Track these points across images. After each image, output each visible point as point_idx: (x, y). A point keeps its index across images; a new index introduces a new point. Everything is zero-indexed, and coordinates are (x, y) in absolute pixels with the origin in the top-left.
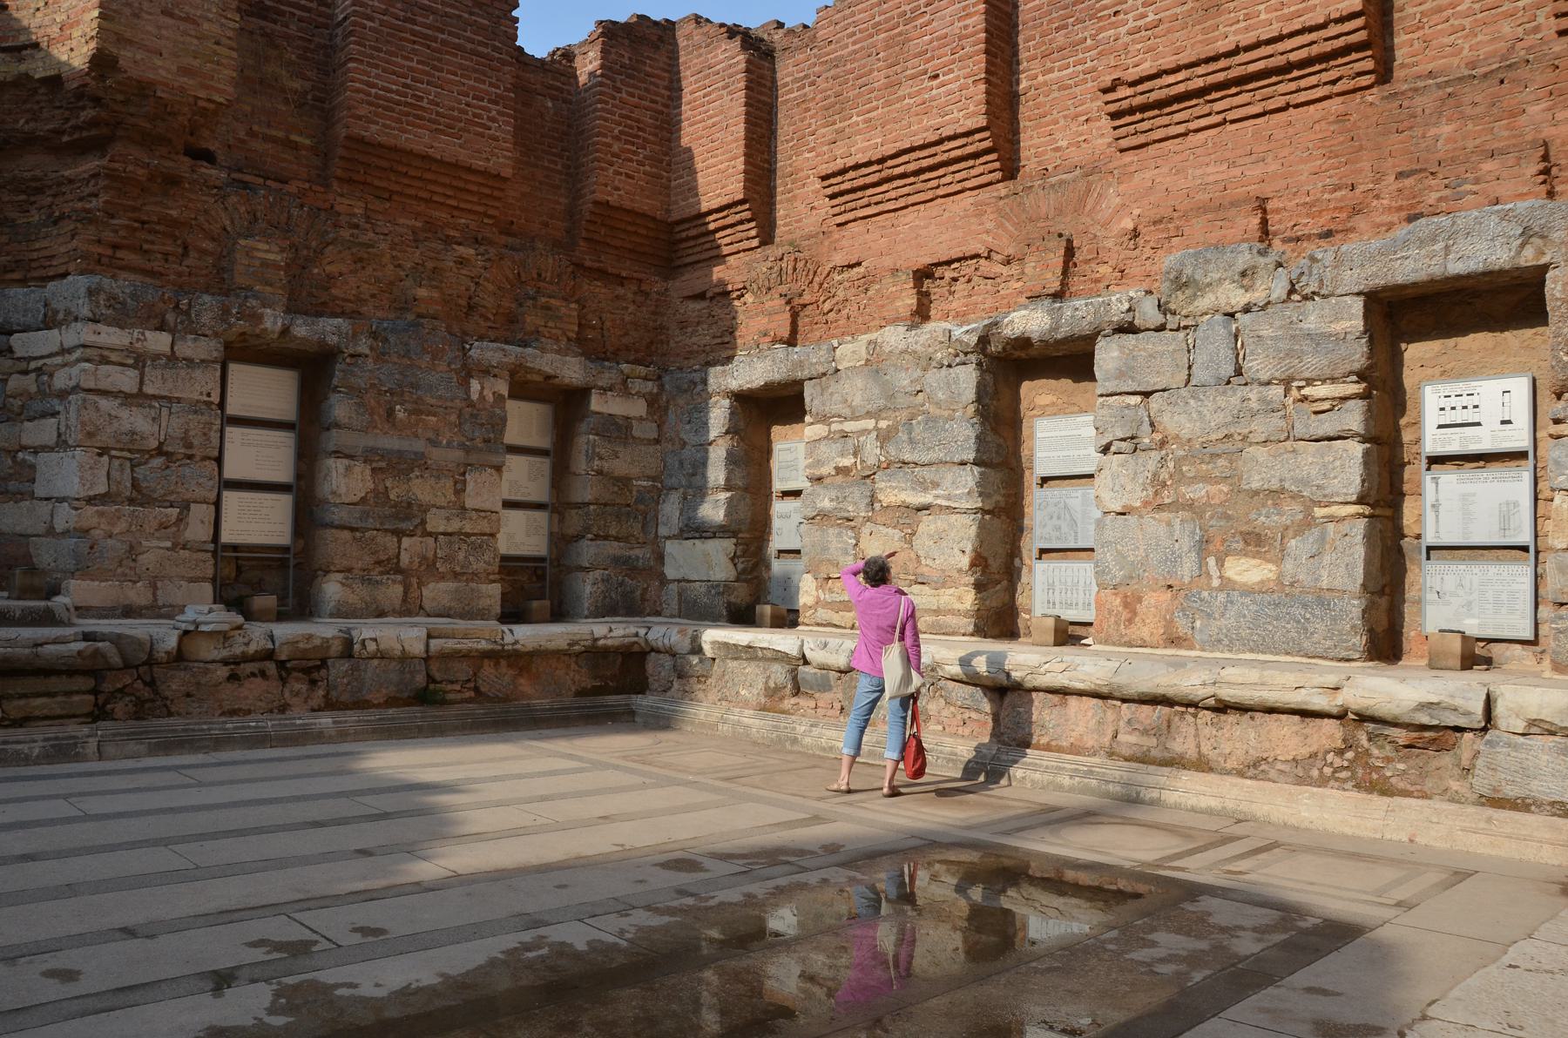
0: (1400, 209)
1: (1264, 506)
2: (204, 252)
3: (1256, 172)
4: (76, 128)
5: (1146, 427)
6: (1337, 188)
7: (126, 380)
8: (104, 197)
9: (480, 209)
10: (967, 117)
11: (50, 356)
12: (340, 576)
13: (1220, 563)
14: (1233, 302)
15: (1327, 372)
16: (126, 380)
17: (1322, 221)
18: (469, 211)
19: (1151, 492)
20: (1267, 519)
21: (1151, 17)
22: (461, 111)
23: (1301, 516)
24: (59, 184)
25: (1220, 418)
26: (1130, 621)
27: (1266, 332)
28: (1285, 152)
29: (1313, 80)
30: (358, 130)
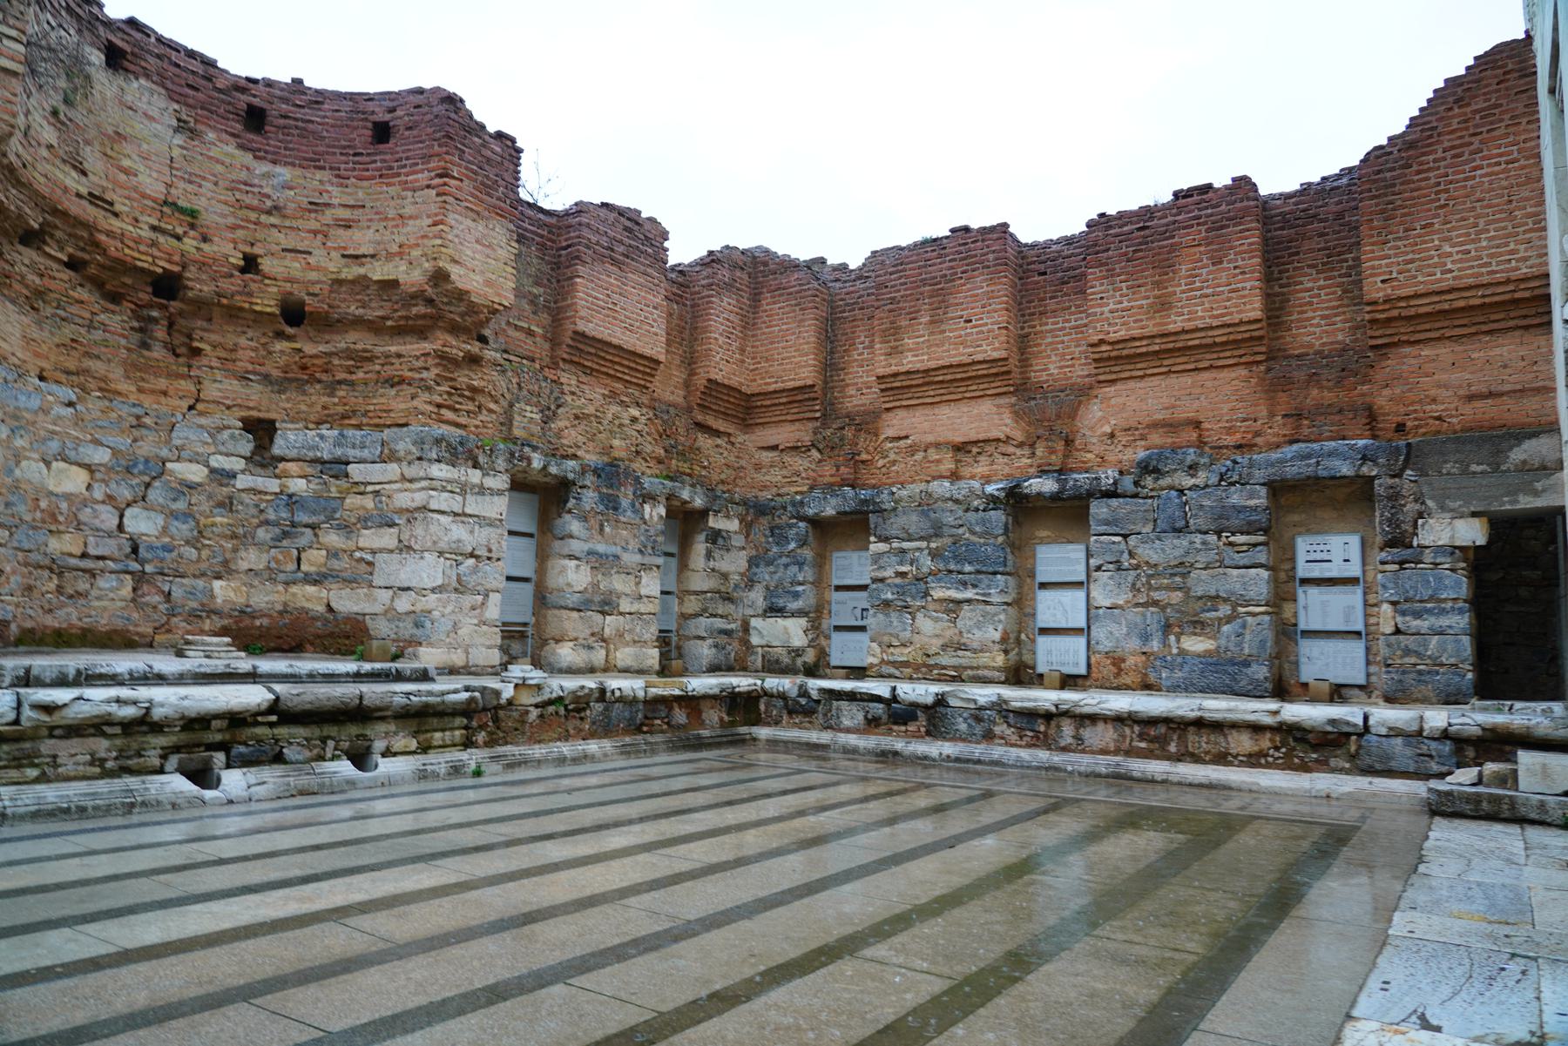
2: (490, 411)
4: (407, 318)
5: (1126, 555)
6: (1244, 420)
7: (455, 503)
8: (435, 371)
10: (995, 349)
11: (390, 482)
12: (571, 644)
13: (1178, 641)
16: (455, 503)
21: (1126, 304)
24: (387, 357)
25: (1177, 553)
29: (1228, 354)
30: (581, 326)
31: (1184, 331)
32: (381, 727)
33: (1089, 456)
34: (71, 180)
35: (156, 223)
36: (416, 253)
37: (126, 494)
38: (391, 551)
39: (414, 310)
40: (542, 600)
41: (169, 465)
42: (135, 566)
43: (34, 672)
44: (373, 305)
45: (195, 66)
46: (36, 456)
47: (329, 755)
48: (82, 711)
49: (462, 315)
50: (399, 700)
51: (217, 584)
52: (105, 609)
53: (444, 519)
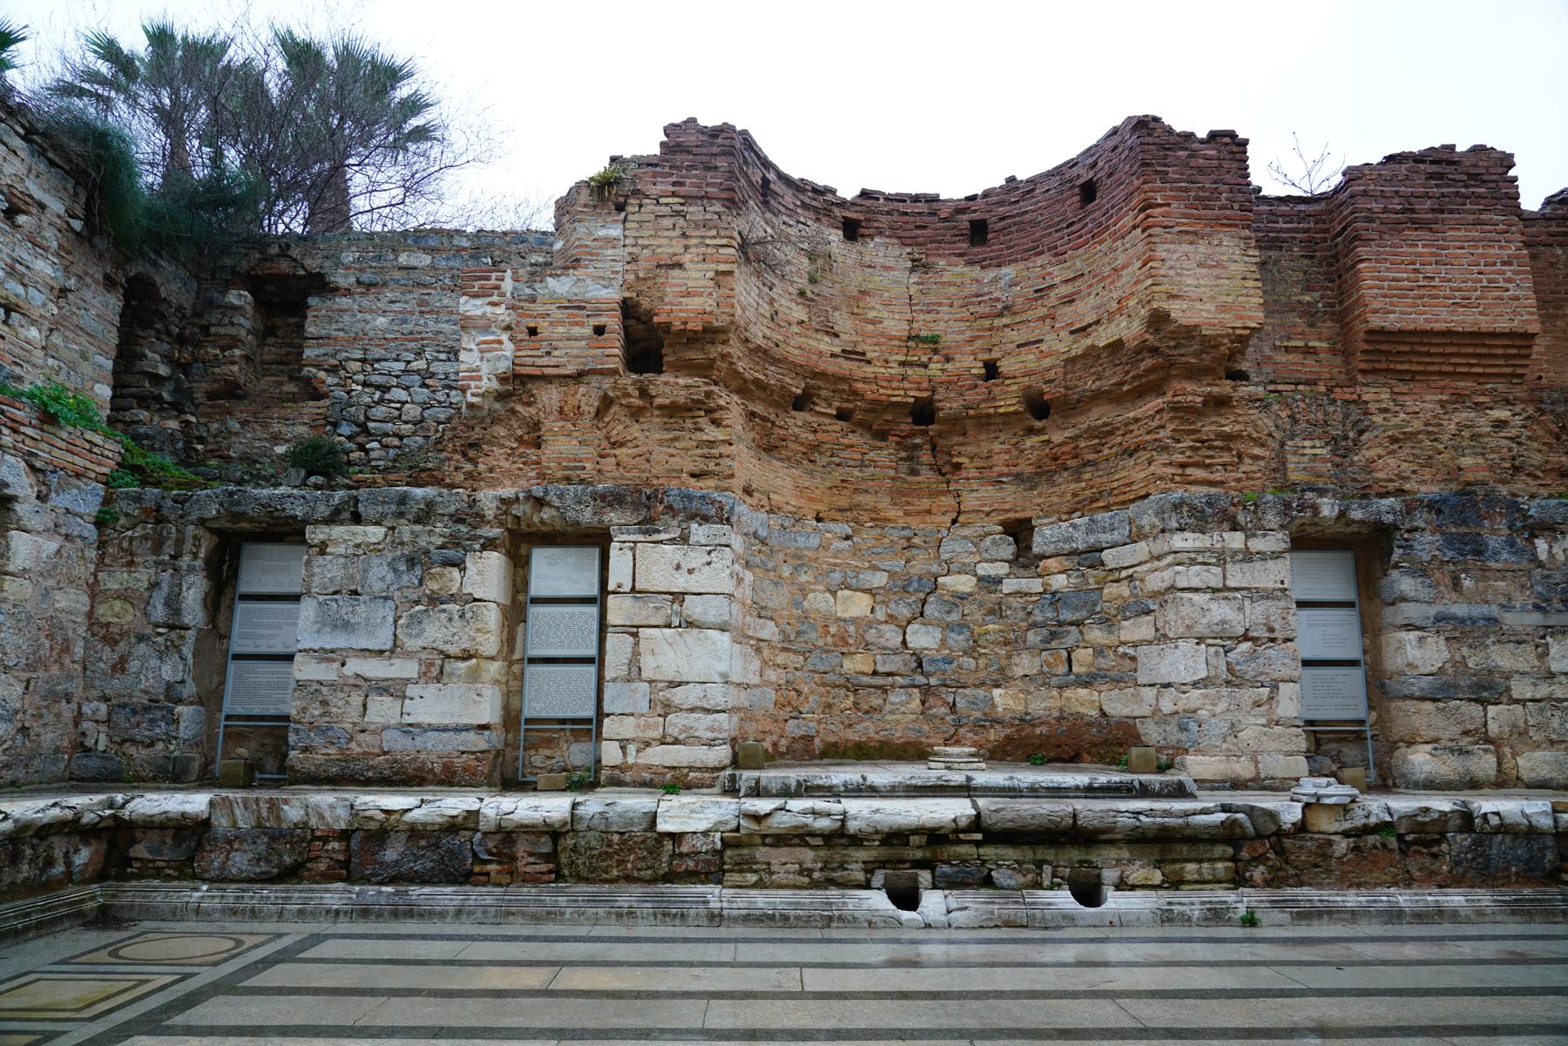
2: (1256, 458)
7: (1213, 577)
8: (1171, 426)
9: (1508, 370)
12: (1428, 747)
16: (1213, 577)
18: (1495, 375)
22: (1474, 281)
24: (1127, 425)
30: (1376, 322)
32: (1112, 853)
34: (826, 344)
35: (903, 358)
36: (1132, 303)
37: (904, 612)
38: (1150, 643)
39: (1143, 366)
40: (1379, 687)
41: (940, 580)
42: (921, 680)
43: (763, 783)
44: (1108, 373)
45: (922, 207)
46: (821, 588)
47: (1046, 883)
48: (782, 822)
49: (1197, 354)
50: (1126, 821)
51: (997, 692)
52: (898, 722)
53: (1197, 598)
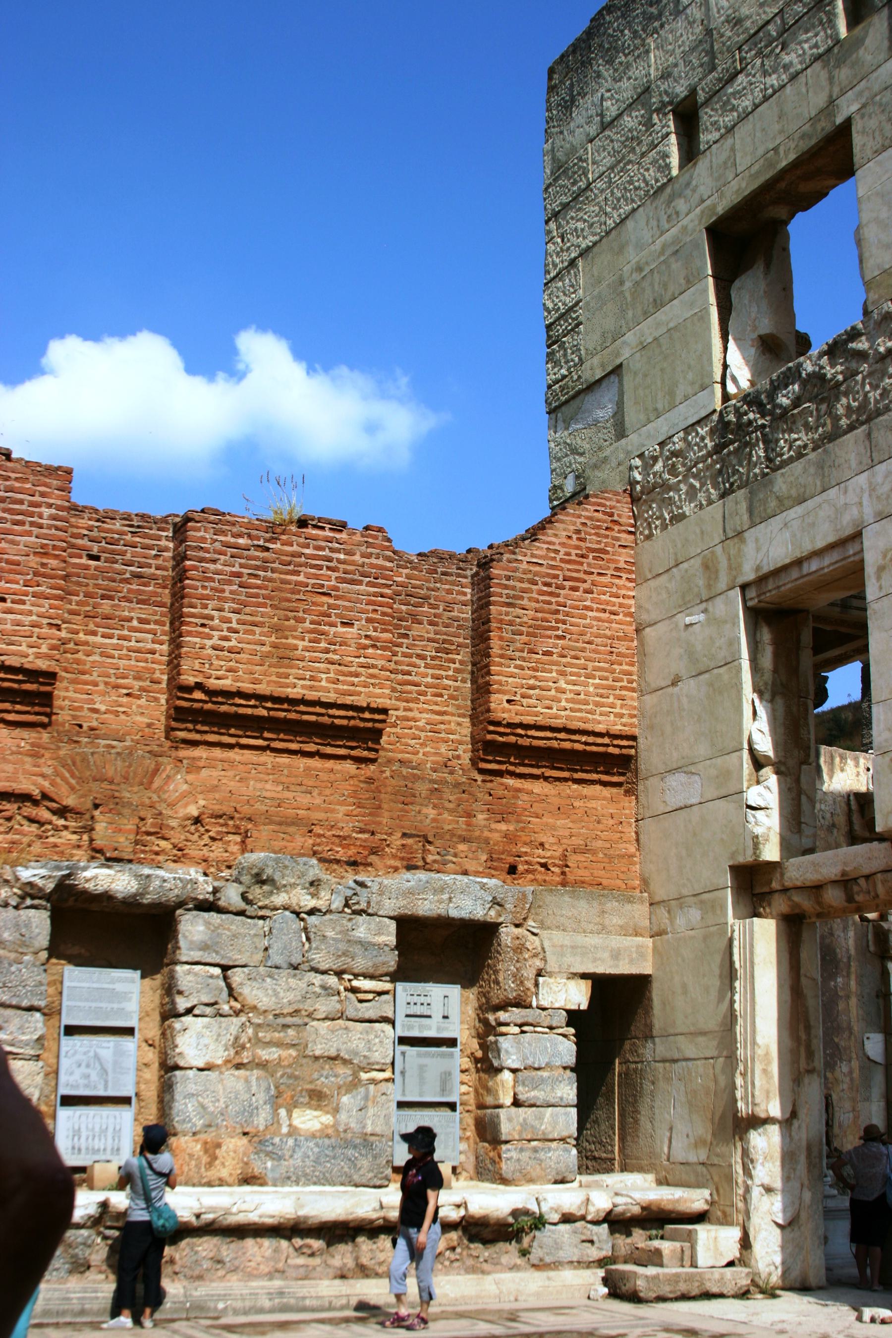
0: (402, 859)
1: (323, 1068)
3: (305, 800)
6: (362, 831)
10: (38, 656)
14: (302, 904)
15: (371, 971)
17: (350, 853)
19: (232, 1052)
20: (328, 1079)
21: (233, 643)
23: (350, 1078)
25: (291, 996)
26: (210, 1164)
27: (330, 934)
28: (328, 792)
31: (303, 701)
33: (163, 844)
